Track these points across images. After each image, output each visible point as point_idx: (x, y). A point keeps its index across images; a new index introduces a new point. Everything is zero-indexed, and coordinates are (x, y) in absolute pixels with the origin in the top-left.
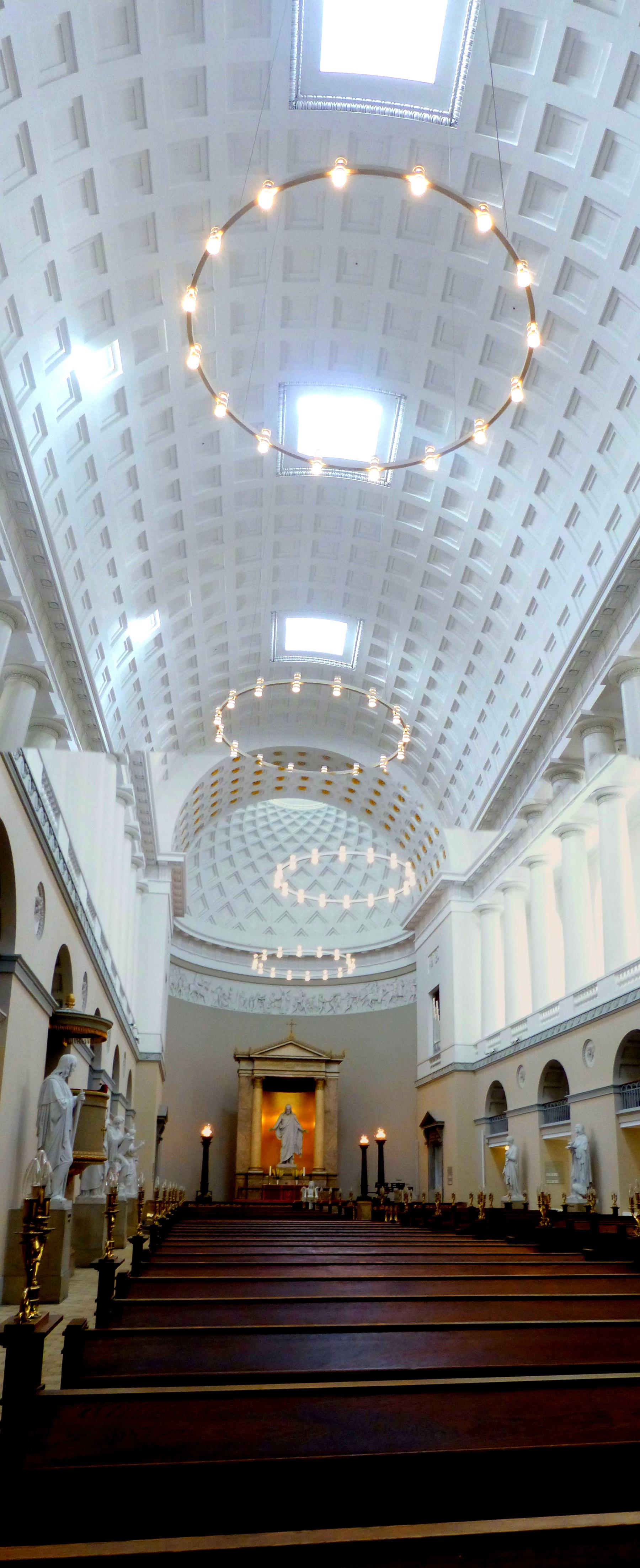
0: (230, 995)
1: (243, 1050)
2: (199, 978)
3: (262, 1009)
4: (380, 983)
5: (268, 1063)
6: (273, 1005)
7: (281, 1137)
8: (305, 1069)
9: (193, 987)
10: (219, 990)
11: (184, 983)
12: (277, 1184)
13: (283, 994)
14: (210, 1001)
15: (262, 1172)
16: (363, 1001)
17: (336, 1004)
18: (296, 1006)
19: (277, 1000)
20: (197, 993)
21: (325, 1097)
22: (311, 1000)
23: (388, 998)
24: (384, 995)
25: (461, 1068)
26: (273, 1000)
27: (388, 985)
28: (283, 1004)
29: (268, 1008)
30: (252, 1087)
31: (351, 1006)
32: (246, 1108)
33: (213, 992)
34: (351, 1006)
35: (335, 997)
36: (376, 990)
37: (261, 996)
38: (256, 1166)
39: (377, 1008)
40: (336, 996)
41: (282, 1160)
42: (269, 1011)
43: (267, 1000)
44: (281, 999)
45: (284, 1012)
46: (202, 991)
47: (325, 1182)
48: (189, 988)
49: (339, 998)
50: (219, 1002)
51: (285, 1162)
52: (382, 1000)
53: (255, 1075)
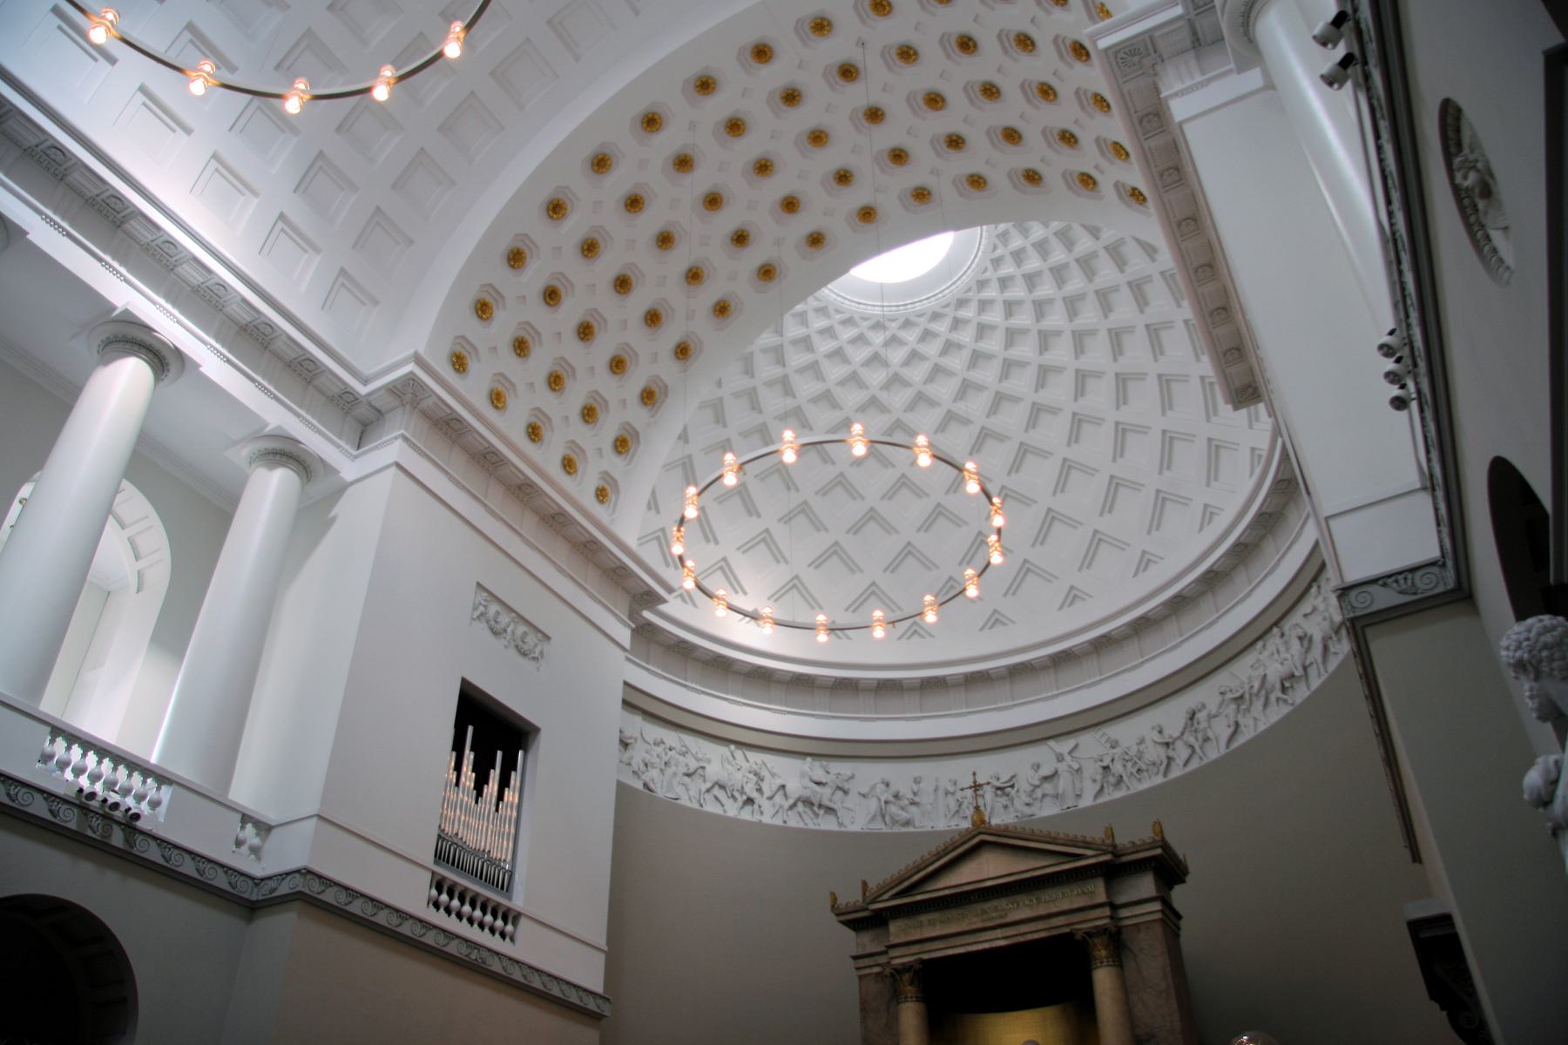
0: (915, 794)
1: (851, 896)
2: (817, 770)
3: (1011, 809)
4: (1287, 625)
5: (924, 918)
6: (1039, 793)
8: (1041, 911)
9: (795, 787)
10: (881, 787)
11: (765, 786)
13: (1060, 758)
14: (857, 818)
16: (1263, 692)
17: (1200, 736)
18: (1098, 777)
19: (1046, 779)
20: (813, 804)
21: (1126, 990)
22: (1133, 751)
23: (1317, 651)
24: (1308, 650)
25: (1385, 598)
26: (1037, 783)
27: (1306, 616)
28: (1064, 783)
29: (1028, 805)
31: (1237, 725)
33: (864, 796)
34: (1237, 725)
35: (1192, 716)
36: (1282, 649)
37: (1004, 778)
39: (1300, 694)
40: (1194, 714)
42: (1028, 811)
43: (1023, 785)
44: (1056, 773)
45: (1070, 803)
46: (824, 794)
48: (786, 796)
49: (1201, 716)
50: (883, 816)
52: (1305, 668)
53: (896, 962)
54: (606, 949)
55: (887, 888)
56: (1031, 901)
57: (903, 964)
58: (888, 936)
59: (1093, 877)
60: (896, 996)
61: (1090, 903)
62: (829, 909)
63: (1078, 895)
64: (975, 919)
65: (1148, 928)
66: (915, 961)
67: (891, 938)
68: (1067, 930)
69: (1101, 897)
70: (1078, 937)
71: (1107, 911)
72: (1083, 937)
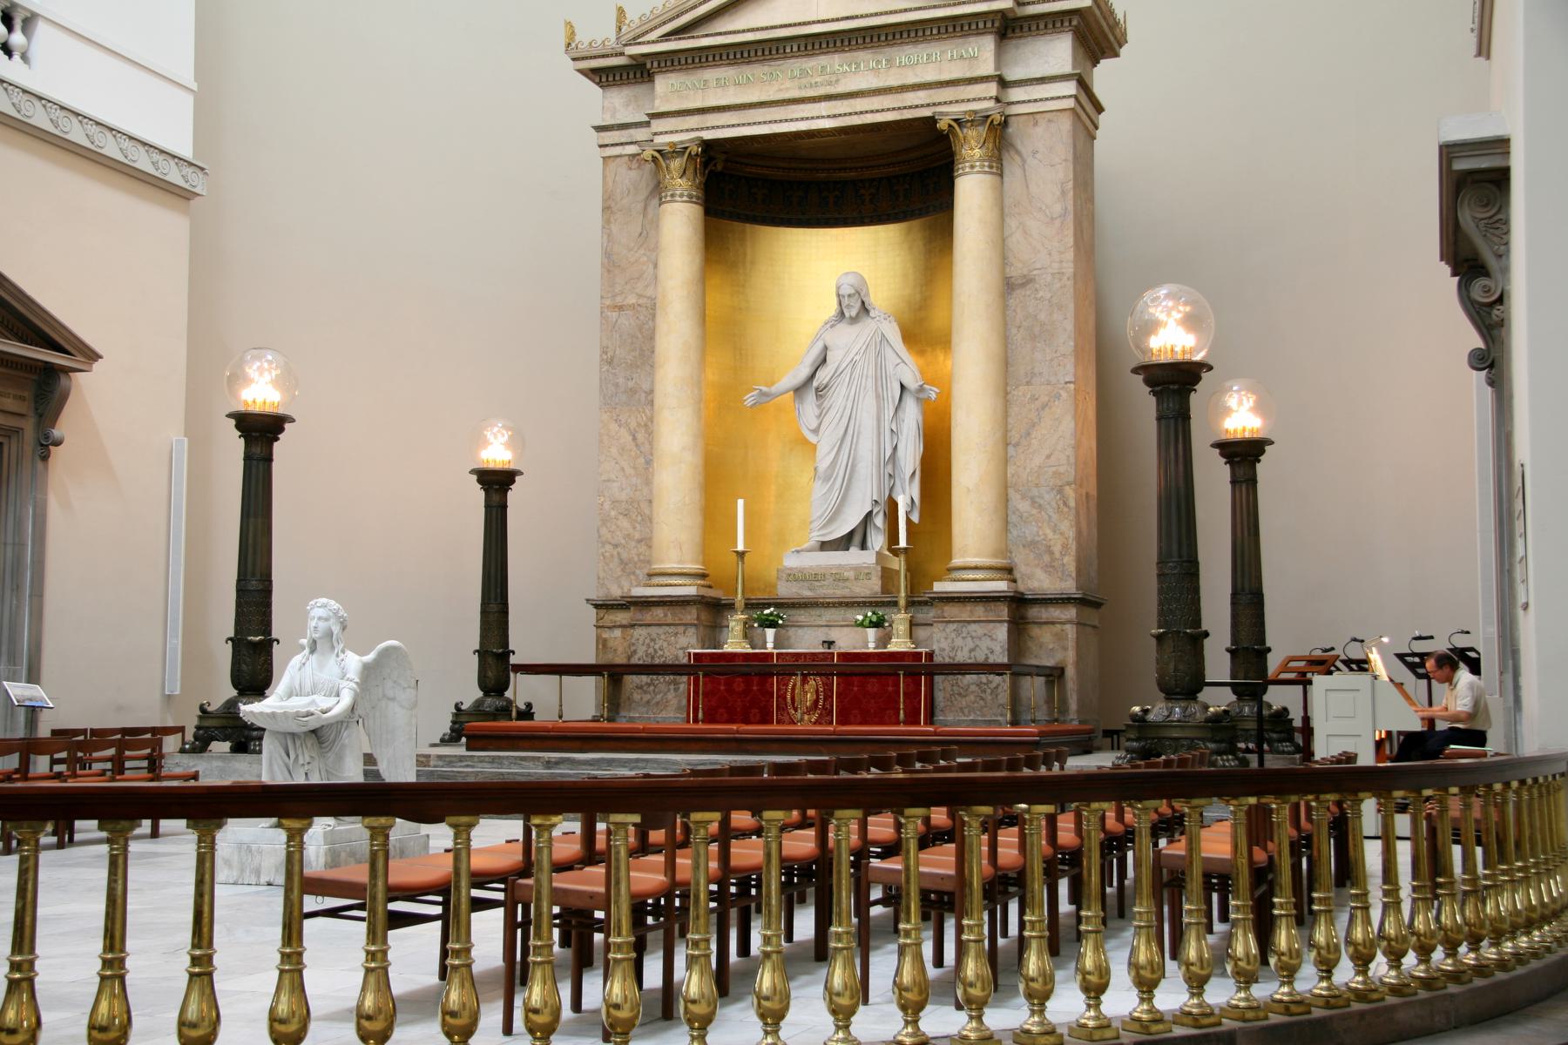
1: (599, 32)
5: (710, 74)
7: (816, 431)
8: (893, 80)
12: (770, 645)
15: (689, 590)
21: (1002, 209)
30: (655, 202)
32: (632, 300)
38: (670, 565)
41: (817, 536)
47: (1002, 632)
51: (844, 543)
53: (659, 140)
54: (194, 86)
55: (657, 21)
56: (878, 62)
57: (673, 144)
58: (653, 100)
59: (979, 33)
60: (658, 191)
61: (968, 75)
62: (563, 48)
63: (952, 59)
64: (788, 84)
65: (1049, 121)
66: (691, 140)
67: (657, 103)
68: (927, 113)
69: (988, 68)
70: (942, 125)
71: (992, 89)
72: (950, 126)
